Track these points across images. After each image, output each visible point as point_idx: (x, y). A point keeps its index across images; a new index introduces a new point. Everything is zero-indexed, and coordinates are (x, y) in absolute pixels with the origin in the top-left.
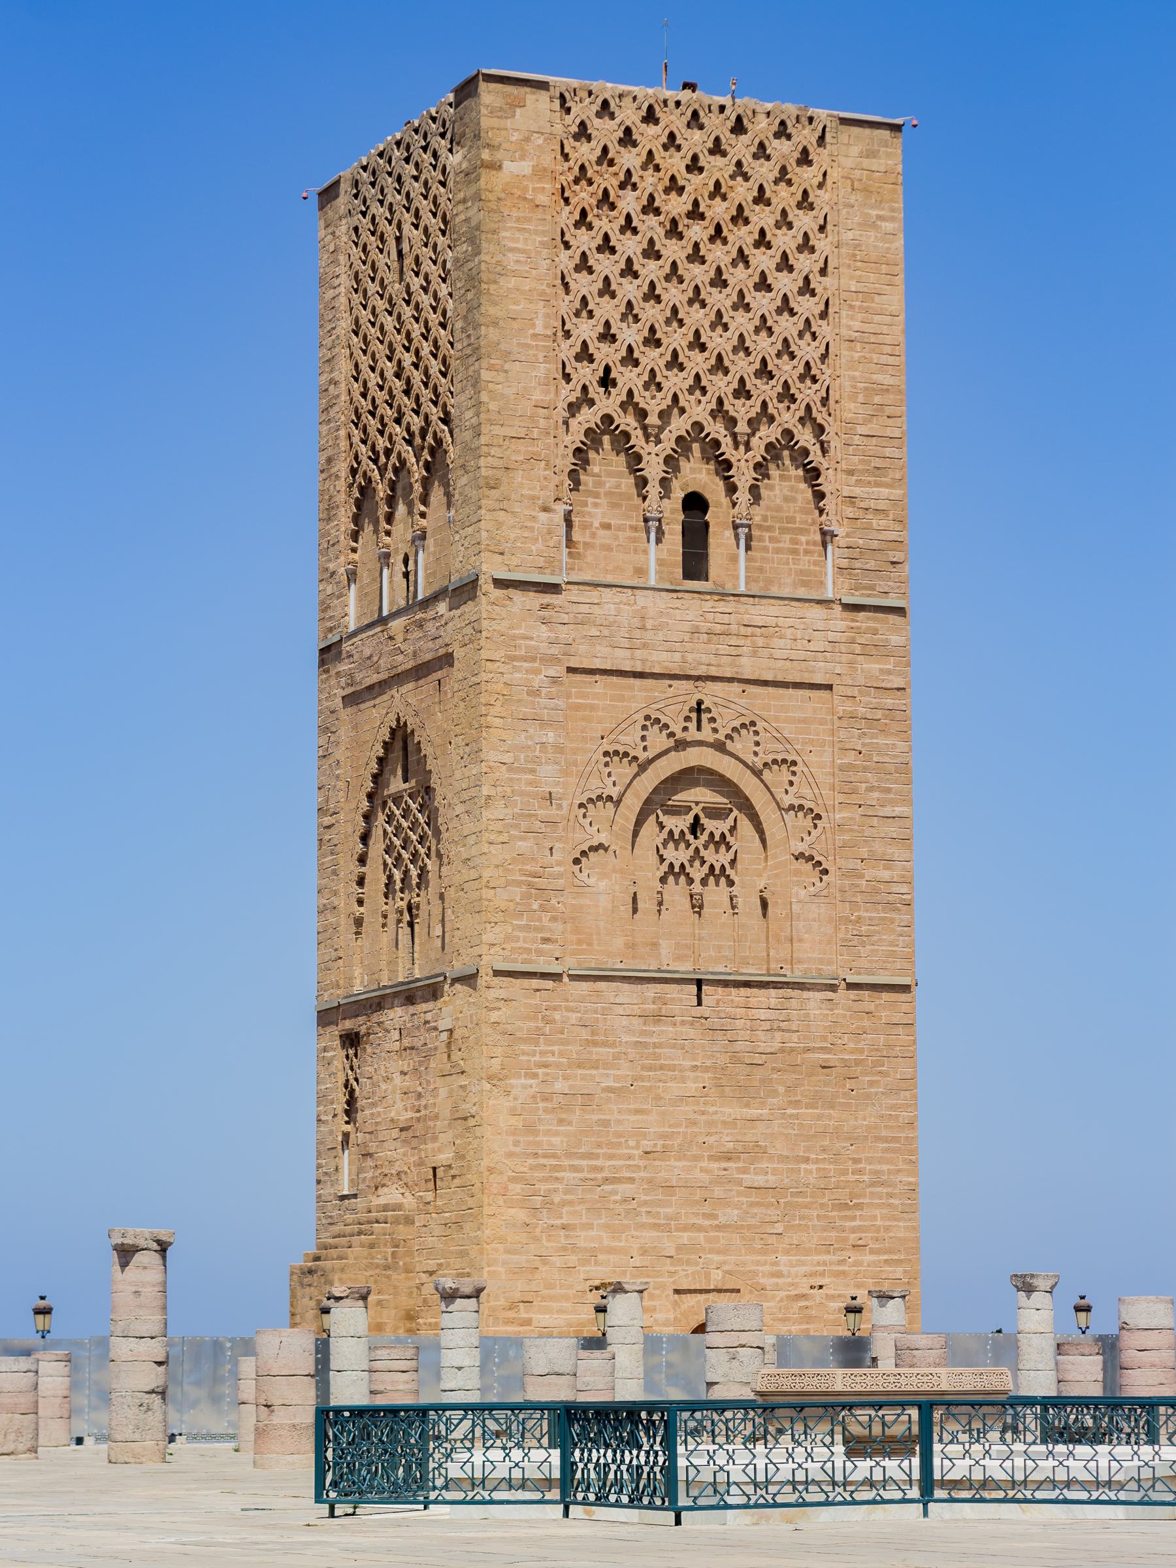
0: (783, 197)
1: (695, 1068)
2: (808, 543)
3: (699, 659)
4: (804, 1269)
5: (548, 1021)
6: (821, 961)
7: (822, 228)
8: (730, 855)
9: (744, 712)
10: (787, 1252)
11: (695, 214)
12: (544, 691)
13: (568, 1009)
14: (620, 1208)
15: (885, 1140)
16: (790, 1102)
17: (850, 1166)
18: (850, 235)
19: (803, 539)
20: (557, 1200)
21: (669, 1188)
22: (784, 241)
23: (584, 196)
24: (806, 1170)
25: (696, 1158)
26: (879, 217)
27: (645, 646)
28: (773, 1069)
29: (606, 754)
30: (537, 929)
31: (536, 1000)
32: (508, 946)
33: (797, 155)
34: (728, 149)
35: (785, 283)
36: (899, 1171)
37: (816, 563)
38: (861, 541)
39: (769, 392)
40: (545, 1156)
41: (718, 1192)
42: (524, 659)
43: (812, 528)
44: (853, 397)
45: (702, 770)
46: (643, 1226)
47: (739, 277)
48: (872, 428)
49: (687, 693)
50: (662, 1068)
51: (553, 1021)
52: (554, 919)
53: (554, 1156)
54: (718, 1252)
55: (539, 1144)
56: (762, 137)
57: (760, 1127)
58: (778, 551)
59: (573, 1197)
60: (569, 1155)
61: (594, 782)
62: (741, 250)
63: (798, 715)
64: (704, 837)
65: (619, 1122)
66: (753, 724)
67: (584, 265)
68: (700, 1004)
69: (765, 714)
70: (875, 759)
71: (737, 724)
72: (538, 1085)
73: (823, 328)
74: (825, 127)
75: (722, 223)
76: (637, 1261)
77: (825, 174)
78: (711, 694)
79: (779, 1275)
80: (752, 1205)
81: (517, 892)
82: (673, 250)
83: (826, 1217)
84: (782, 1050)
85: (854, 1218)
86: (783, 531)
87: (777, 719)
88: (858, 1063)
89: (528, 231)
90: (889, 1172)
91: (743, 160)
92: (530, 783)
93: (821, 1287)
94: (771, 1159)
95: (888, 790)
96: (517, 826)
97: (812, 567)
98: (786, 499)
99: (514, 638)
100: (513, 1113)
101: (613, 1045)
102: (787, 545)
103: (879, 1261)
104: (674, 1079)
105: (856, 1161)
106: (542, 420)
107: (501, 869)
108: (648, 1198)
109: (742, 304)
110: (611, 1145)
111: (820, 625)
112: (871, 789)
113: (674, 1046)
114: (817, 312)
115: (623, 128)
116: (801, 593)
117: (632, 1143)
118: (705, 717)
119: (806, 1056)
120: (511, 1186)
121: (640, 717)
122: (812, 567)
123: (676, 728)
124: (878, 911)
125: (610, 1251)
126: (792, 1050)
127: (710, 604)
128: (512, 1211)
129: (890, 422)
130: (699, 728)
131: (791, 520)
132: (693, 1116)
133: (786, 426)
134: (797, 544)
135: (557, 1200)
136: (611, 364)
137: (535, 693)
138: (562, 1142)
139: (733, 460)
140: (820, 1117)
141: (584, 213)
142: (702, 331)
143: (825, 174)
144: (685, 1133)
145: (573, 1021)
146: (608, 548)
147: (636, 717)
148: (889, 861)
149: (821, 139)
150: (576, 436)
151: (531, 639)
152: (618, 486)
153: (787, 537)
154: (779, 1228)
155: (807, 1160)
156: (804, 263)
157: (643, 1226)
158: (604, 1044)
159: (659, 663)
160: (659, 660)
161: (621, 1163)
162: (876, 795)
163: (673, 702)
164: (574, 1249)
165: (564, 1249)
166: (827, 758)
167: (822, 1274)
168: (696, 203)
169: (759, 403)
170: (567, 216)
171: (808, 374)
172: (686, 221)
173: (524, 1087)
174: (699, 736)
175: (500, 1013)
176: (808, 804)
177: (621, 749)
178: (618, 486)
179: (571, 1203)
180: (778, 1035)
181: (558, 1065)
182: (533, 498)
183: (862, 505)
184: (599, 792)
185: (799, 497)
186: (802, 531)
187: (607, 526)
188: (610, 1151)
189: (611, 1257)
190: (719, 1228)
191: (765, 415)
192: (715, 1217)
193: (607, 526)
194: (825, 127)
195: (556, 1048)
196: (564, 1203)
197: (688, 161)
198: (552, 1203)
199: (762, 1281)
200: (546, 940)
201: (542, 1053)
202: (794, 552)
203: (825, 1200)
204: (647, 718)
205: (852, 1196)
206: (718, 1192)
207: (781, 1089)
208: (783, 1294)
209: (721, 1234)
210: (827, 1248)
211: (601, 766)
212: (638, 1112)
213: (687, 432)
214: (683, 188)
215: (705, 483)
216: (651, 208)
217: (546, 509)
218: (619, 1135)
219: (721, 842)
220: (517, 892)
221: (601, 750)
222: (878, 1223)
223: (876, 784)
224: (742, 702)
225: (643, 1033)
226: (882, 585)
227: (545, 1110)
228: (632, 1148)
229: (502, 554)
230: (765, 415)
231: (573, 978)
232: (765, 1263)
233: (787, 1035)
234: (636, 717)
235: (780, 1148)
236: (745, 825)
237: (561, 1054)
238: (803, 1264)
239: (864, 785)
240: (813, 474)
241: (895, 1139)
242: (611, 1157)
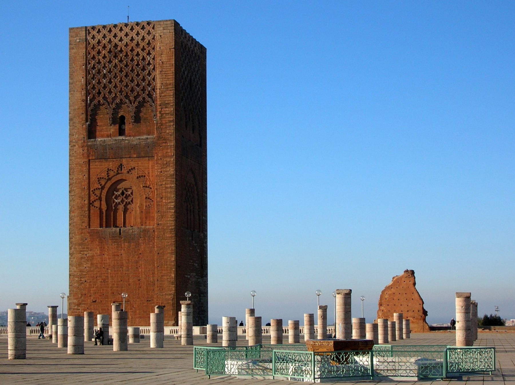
7: (154, 49)
29: (98, 178)
64: (124, 195)
118: (123, 167)
121: (106, 169)
130: (121, 170)
149: (153, 28)
191: (138, 95)
230: (138, 95)
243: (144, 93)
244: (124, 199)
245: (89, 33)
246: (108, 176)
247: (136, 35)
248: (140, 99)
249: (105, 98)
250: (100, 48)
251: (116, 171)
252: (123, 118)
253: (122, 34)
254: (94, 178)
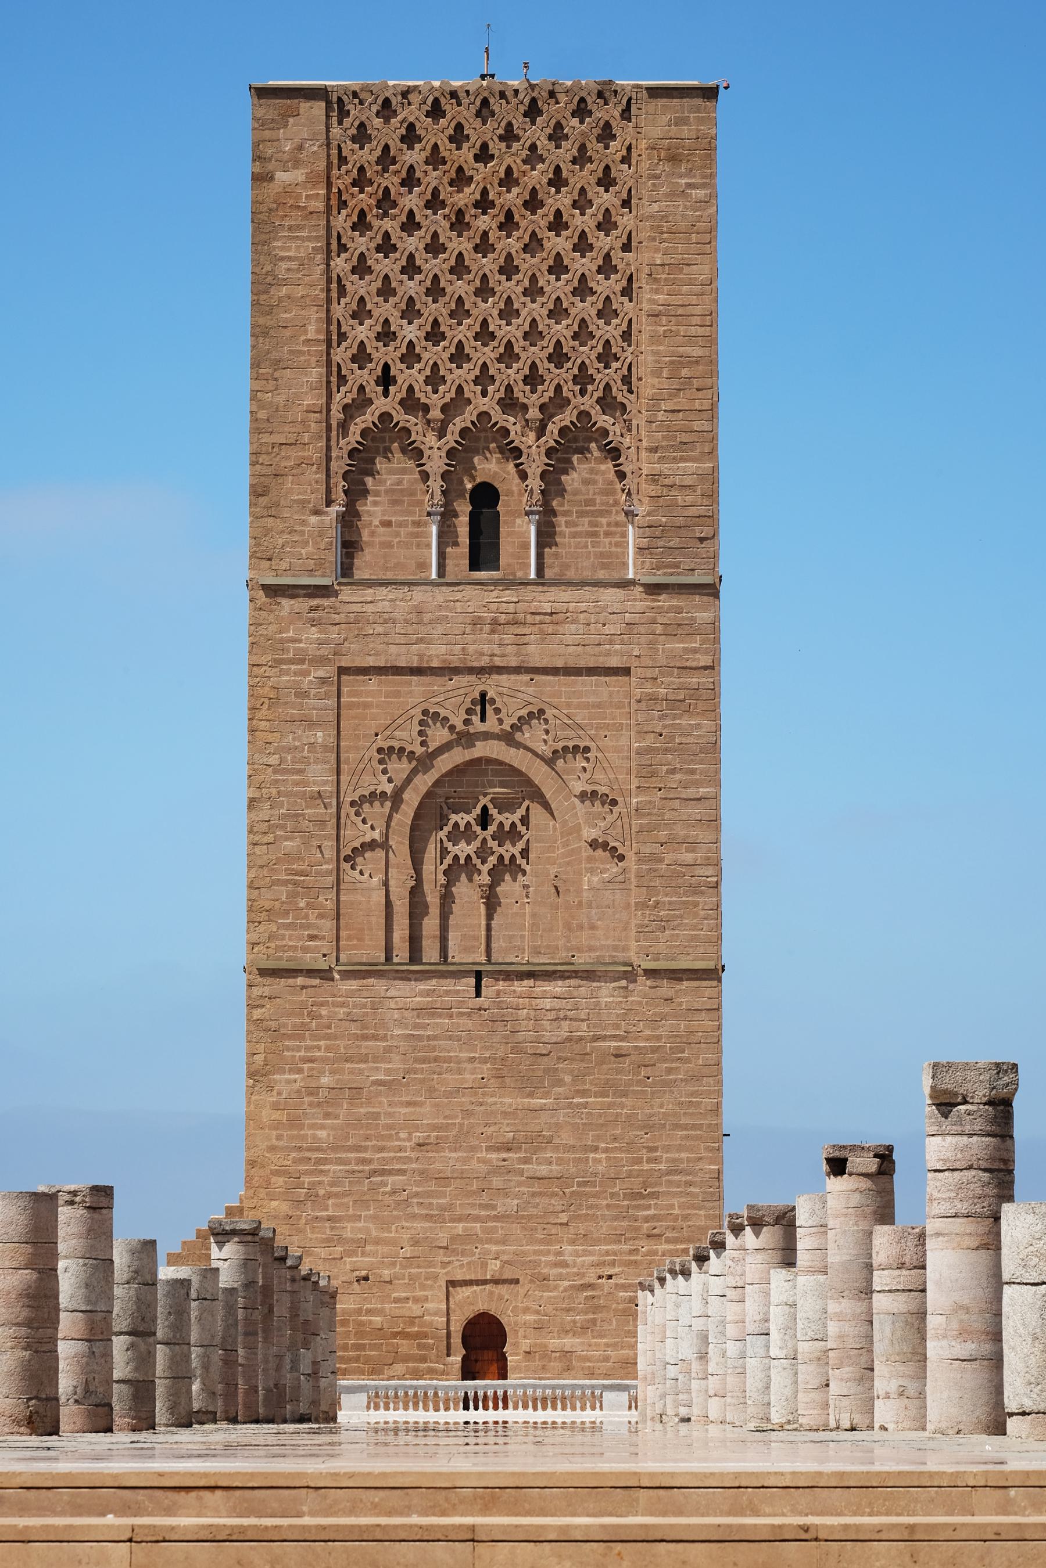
0: (584, 177)
1: (472, 1060)
2: (609, 525)
3: (481, 648)
4: (591, 1258)
5: (312, 1015)
6: (615, 948)
7: (626, 203)
8: (521, 845)
9: (532, 700)
10: (573, 1242)
11: (484, 204)
12: (313, 692)
13: (334, 1005)
14: (389, 1200)
15: (685, 1127)
16: (578, 1091)
18: (656, 207)
19: (604, 521)
20: (321, 1192)
21: (443, 1180)
22: (583, 222)
23: (364, 199)
24: (595, 1160)
25: (473, 1149)
26: (689, 185)
27: (421, 641)
28: (559, 1058)
29: (380, 750)
30: (303, 927)
31: (303, 996)
32: (273, 945)
33: (597, 131)
34: (521, 133)
35: (584, 264)
36: (700, 1158)
37: (617, 544)
38: (664, 519)
39: (564, 375)
40: (309, 1150)
41: (497, 1182)
42: (292, 662)
43: (614, 509)
44: (657, 373)
45: (489, 761)
46: (414, 1217)
47: (527, 263)
48: (681, 401)
49: (468, 686)
50: (436, 1060)
51: (320, 1016)
52: (321, 916)
53: (318, 1149)
54: (497, 1243)
55: (304, 1138)
56: (559, 116)
57: (545, 1117)
58: (574, 535)
59: (339, 1189)
60: (335, 1148)
61: (367, 779)
62: (534, 234)
63: (592, 699)
64: (492, 828)
65: (390, 1115)
66: (541, 712)
67: (361, 268)
68: (478, 994)
69: (555, 701)
70: (677, 741)
71: (524, 712)
72: (303, 1079)
73: (625, 307)
74: (630, 99)
75: (513, 209)
76: (408, 1251)
77: (629, 148)
78: (492, 685)
79: (564, 1264)
81: (283, 892)
82: (460, 244)
83: (618, 1206)
84: (569, 1039)
85: (649, 1207)
86: (581, 514)
87: (569, 705)
88: (654, 1050)
89: (302, 239)
90: (689, 1160)
91: (538, 143)
92: (297, 784)
93: (610, 1277)
94: (556, 1149)
95: (693, 772)
96: (283, 827)
97: (613, 549)
98: (586, 482)
99: (282, 641)
100: (276, 1106)
101: (384, 1038)
102: (587, 528)
103: (677, 1250)
104: (449, 1070)
105: (654, 1149)
106: (313, 425)
107: (266, 869)
108: (419, 1189)
109: (533, 291)
110: (382, 1138)
111: (617, 607)
112: (673, 771)
113: (450, 1038)
114: (618, 288)
115: (405, 125)
116: (602, 575)
117: (402, 1135)
118: (489, 708)
119: (595, 1044)
120: (274, 1179)
121: (417, 713)
122: (613, 549)
123: (458, 722)
124: (678, 895)
125: (377, 1242)
126: (581, 1039)
127: (495, 593)
128: (274, 1204)
129: (700, 394)
130: (483, 719)
131: (590, 502)
132: (470, 1107)
133: (582, 408)
134: (596, 526)
135: (321, 1192)
136: (390, 362)
137: (305, 694)
138: (329, 1135)
139: (522, 447)
140: (610, 1105)
141: (362, 214)
142: (490, 320)
143: (629, 148)
144: (461, 1125)
145: (341, 1016)
146: (389, 545)
147: (412, 712)
148: (692, 846)
150: (354, 436)
151: (300, 641)
152: (400, 482)
153: (587, 520)
154: (563, 1218)
155: (596, 1149)
156: (602, 242)
157: (414, 1217)
158: (375, 1038)
159: (437, 656)
160: (437, 654)
161: (392, 1154)
162: (678, 777)
163: (453, 697)
164: (341, 1240)
165: (328, 1240)
166: (624, 742)
167: (613, 1264)
168: (485, 192)
169: (552, 388)
170: (342, 221)
171: (606, 357)
172: (473, 211)
173: (288, 1082)
174: (481, 727)
175: (263, 1010)
176: (602, 790)
177: (397, 745)
178: (400, 482)
179: (337, 1195)
180: (565, 1024)
181: (324, 1060)
182: (303, 502)
183: (667, 482)
184: (372, 788)
185: (600, 479)
186: (602, 513)
187: (387, 524)
188: (379, 1144)
189: (379, 1247)
190: (496, 1218)
191: (558, 401)
192: (494, 1207)
193: (387, 524)
194: (630, 99)
195: (321, 1043)
196: (329, 1196)
197: (476, 150)
198: (317, 1196)
199: (545, 1271)
200: (312, 938)
201: (308, 1049)
202: (595, 534)
203: (616, 1190)
204: (425, 712)
206: (497, 1182)
207: (568, 1079)
208: (566, 1283)
209: (499, 1224)
210: (618, 1238)
211: (375, 763)
212: (409, 1104)
213: (472, 422)
214: (472, 177)
215: (496, 473)
216: (434, 202)
217: (317, 512)
218: (389, 1127)
219: (512, 834)
220: (283, 892)
221: (375, 747)
222: (676, 1212)
223: (678, 766)
224: (531, 690)
225: (416, 1026)
226: (687, 563)
227: (311, 1104)
228: (404, 1140)
229: (270, 559)
230: (558, 401)
231: (347, 975)
232: (548, 1252)
233: (574, 1023)
234: (412, 712)
235: (566, 1137)
236: (537, 813)
237: (328, 1049)
239: (665, 768)
240: (614, 453)
241: (699, 1127)
242: (382, 1149)
243: (583, 392)
244: (492, 844)
245: (343, 114)
246: (423, 744)
247: (550, 138)
248: (566, 418)
249: (411, 403)
250: (391, 181)
251: (458, 722)
252: (486, 497)
253: (488, 132)
254: (360, 750)
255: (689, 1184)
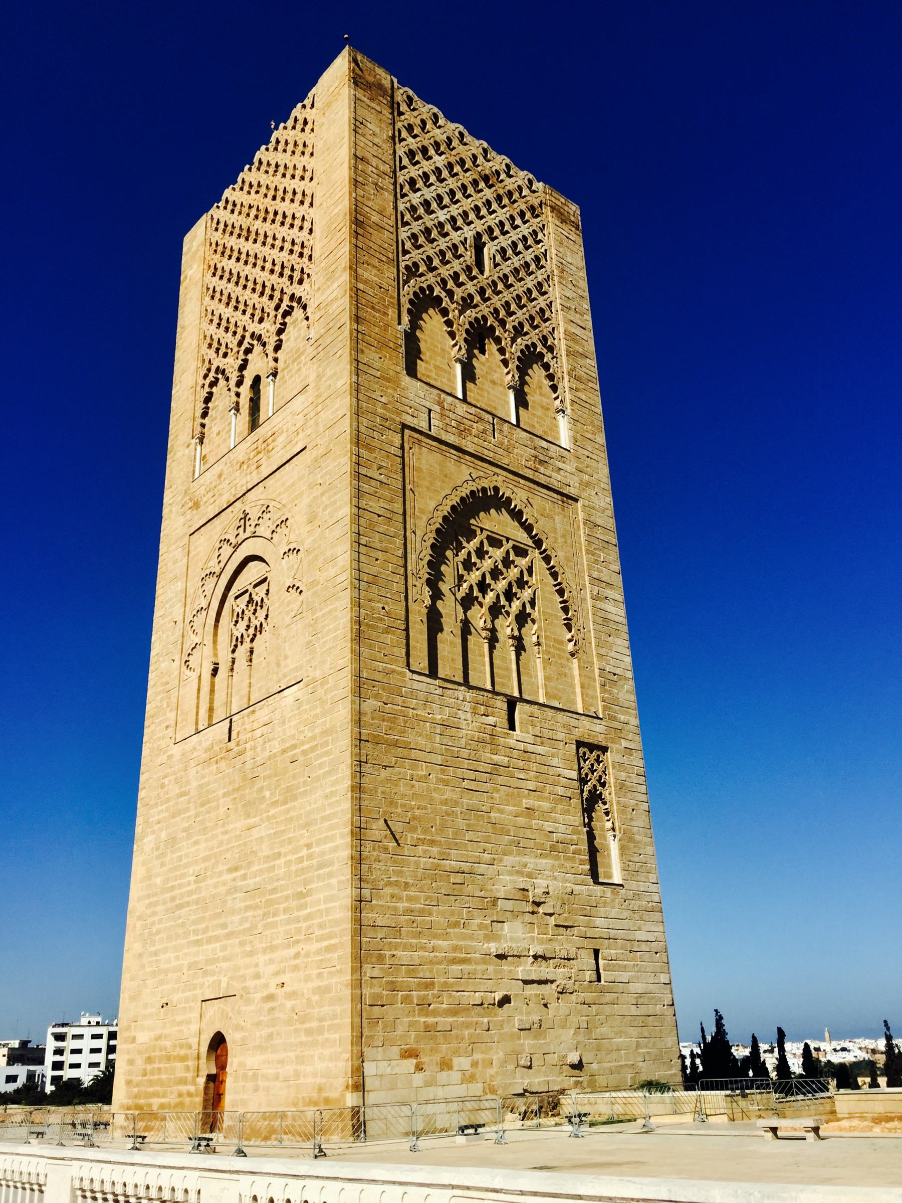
10: (264, 951)
17: (305, 852)
57: (256, 833)
79: (257, 976)
80: (247, 908)
95: (335, 502)
155: (279, 855)
205: (306, 882)
207: (267, 794)
238: (271, 961)
242: (180, 886)
255: (330, 875)
